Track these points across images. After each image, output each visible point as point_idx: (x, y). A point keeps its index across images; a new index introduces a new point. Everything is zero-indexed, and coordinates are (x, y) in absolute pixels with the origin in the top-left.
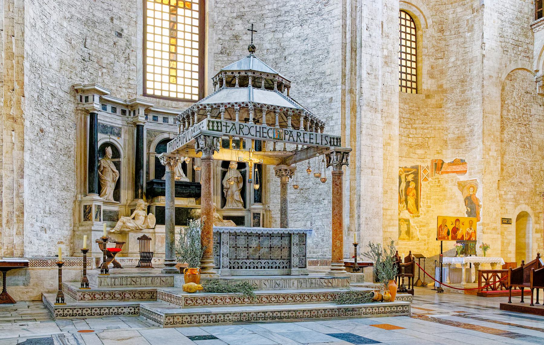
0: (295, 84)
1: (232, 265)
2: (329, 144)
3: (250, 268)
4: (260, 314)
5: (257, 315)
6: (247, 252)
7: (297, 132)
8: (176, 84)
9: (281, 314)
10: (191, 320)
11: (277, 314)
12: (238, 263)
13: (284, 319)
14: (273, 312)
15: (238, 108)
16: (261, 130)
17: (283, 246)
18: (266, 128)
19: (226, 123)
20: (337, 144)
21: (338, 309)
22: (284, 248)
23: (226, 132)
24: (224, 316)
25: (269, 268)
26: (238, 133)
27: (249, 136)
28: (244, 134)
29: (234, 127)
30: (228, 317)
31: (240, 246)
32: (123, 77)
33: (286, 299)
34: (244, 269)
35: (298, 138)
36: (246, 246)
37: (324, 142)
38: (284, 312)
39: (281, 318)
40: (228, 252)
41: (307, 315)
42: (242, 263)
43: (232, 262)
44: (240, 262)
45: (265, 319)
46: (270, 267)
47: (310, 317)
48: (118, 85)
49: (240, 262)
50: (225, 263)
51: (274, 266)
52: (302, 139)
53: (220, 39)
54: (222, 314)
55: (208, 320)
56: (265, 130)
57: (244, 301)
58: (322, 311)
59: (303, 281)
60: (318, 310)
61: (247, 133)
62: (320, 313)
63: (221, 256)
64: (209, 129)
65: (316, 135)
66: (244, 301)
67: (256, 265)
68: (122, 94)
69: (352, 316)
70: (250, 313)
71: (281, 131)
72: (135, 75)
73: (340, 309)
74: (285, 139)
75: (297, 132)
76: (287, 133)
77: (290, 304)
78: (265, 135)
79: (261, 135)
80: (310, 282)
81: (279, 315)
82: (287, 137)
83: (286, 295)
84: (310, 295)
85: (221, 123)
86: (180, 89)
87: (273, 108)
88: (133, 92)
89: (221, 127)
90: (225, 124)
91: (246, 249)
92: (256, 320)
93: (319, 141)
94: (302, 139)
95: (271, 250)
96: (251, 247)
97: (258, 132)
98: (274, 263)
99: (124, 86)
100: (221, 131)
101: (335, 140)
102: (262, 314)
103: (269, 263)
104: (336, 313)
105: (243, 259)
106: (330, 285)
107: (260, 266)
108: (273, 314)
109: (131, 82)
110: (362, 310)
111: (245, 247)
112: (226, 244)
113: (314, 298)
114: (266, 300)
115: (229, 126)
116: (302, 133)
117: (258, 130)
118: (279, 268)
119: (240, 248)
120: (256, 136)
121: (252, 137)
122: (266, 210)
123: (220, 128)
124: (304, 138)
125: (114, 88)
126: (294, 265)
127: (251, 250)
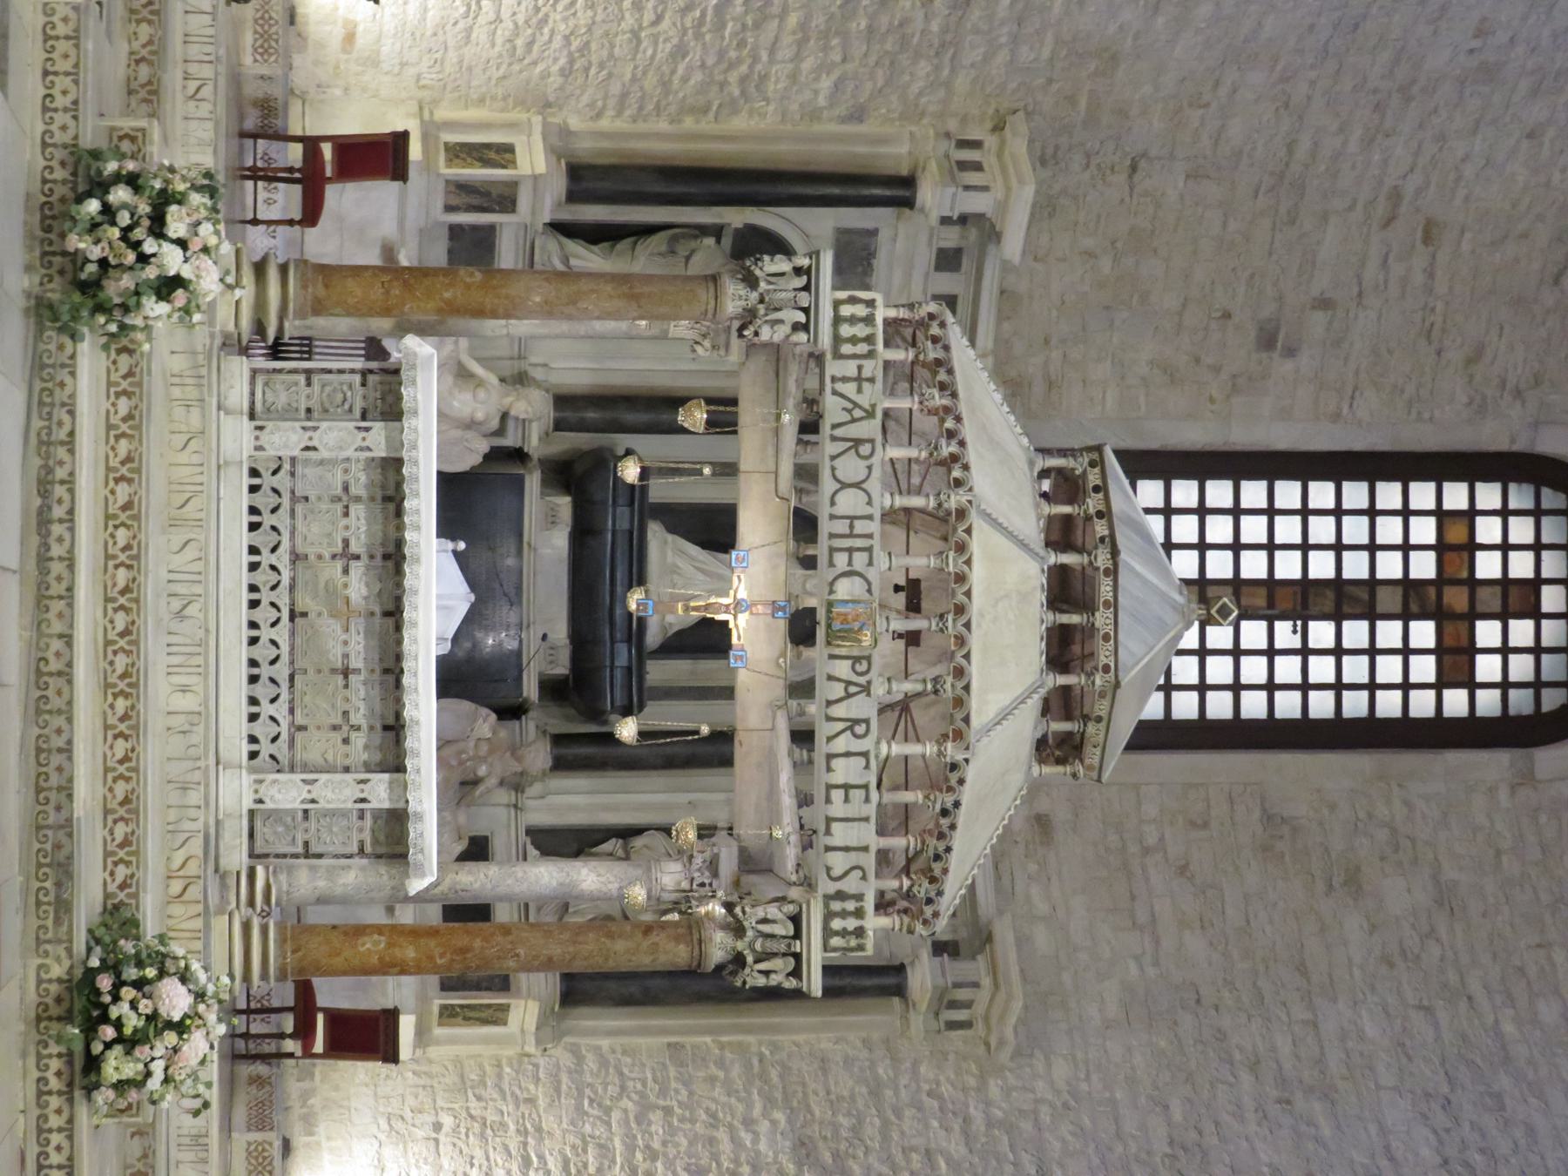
1: (267, 481)
2: (832, 888)
4: (66, 418)
5: (63, 405)
6: (327, 556)
7: (867, 721)
9: (61, 521)
10: (56, 110)
12: (274, 511)
13: (35, 540)
14: (70, 482)
16: (859, 543)
17: (353, 735)
18: (870, 564)
19: (872, 380)
20: (837, 933)
21: (69, 820)
22: (346, 741)
23: (834, 379)
25: (253, 663)
26: (839, 432)
27: (832, 486)
28: (833, 458)
29: (858, 413)
33: (122, 601)
34: (246, 538)
35: (841, 726)
37: (839, 862)
38: (67, 536)
40: (324, 454)
41: (50, 655)
42: (274, 528)
45: (41, 443)
46: (255, 671)
47: (39, 673)
49: (282, 520)
50: (276, 438)
53: (1333, 807)
57: (118, 395)
58: (65, 737)
59: (195, 738)
60: (68, 712)
61: (839, 474)
62: (59, 721)
63: (310, 424)
66: (118, 395)
67: (265, 596)
69: (32, 900)
70: (73, 374)
73: (70, 835)
74: (832, 657)
75: (867, 721)
78: (841, 560)
79: (838, 543)
80: (189, 777)
81: (58, 512)
83: (137, 601)
84: (136, 727)
85: (871, 354)
87: (961, 598)
89: (855, 356)
90: (866, 373)
91: (339, 549)
92: (41, 403)
95: (334, 671)
96: (346, 571)
97: (851, 527)
98: (273, 690)
99: (1056, 355)
102: (67, 428)
103: (273, 662)
104: (50, 808)
105: (293, 533)
106: (176, 887)
107: (257, 615)
108: (62, 482)
110: (58, 960)
111: (346, 542)
112: (359, 443)
114: (121, 502)
115: (859, 390)
117: (860, 527)
119: (344, 522)
120: (832, 517)
121: (827, 501)
123: (846, 349)
124: (848, 754)
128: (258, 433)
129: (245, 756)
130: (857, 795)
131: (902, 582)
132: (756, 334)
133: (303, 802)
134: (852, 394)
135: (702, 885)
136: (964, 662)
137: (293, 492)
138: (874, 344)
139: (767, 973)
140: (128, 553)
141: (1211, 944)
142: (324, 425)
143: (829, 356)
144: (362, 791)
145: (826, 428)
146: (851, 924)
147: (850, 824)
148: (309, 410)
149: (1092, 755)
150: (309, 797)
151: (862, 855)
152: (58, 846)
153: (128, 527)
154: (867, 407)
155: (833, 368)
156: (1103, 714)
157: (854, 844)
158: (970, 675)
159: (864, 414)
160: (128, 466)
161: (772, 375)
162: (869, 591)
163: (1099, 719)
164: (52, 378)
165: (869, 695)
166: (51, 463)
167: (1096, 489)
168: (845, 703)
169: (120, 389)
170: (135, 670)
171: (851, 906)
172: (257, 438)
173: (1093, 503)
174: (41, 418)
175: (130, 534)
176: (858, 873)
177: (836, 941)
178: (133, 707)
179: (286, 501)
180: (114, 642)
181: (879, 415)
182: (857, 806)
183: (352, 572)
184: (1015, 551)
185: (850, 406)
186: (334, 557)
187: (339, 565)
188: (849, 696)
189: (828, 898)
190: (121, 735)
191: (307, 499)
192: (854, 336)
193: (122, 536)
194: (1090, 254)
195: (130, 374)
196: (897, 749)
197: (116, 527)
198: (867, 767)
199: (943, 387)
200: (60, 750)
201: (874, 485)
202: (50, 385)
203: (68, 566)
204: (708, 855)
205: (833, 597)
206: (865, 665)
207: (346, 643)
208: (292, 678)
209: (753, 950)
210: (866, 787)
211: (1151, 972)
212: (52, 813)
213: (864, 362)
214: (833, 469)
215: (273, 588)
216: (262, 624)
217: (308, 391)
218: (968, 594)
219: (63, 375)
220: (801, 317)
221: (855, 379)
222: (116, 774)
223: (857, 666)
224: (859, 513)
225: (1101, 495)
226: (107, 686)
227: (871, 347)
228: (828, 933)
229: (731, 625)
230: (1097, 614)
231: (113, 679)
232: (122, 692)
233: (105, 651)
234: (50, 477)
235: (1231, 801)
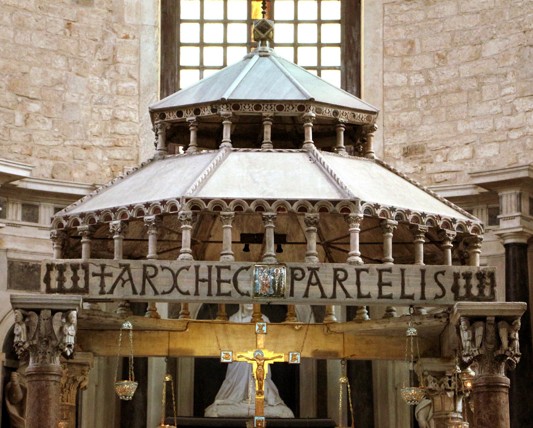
2: (450, 294)
7: (336, 270)
16: (214, 276)
18: (229, 268)
19: (103, 267)
26: (139, 289)
28: (156, 293)
29: (126, 276)
32: (95, 116)
35: (339, 288)
48: (78, 143)
61: (167, 289)
68: (92, 167)
72: (135, 107)
74: (292, 294)
76: (300, 275)
78: (226, 288)
79: (214, 290)
85: (85, 267)
87: (252, 207)
88: (128, 157)
89: (86, 278)
90: (98, 270)
94: (352, 288)
97: (203, 280)
99: (98, 142)
109: (121, 127)
115: (110, 275)
116: (351, 271)
117: (203, 275)
120: (197, 293)
121: (185, 297)
123: (81, 284)
124: (358, 284)
125: (62, 154)
130: (386, 277)
131: (243, 246)
132: (69, 346)
134: (114, 279)
135: (450, 383)
136: (295, 205)
138: (78, 265)
139: (511, 341)
141: (492, 38)
143: (86, 296)
145: (137, 297)
146: (474, 282)
147: (406, 283)
149: (361, 118)
151: (427, 274)
155: (94, 293)
156: (332, 110)
157: (420, 279)
158: (304, 200)
159: (126, 273)
161: (102, 334)
162: (247, 268)
163: (336, 113)
165: (317, 269)
168: (323, 285)
171: (462, 282)
173: (190, 117)
176: (440, 277)
177: (487, 292)
181: (127, 261)
182: (394, 278)
184: (221, 170)
185: (121, 282)
188: (318, 283)
192: (72, 278)
194: (27, 118)
196: (356, 249)
198: (367, 270)
199: (109, 218)
201: (175, 265)
204: (430, 378)
205: (251, 294)
206: (296, 272)
209: (494, 350)
210: (380, 271)
211: (511, 78)
213: (91, 272)
214: (164, 293)
218: (249, 201)
221: (102, 278)
223: (298, 277)
224: (194, 276)
225: (184, 113)
227: (80, 267)
228: (480, 297)
229: (272, 362)
230: (264, 114)
235: (395, 26)
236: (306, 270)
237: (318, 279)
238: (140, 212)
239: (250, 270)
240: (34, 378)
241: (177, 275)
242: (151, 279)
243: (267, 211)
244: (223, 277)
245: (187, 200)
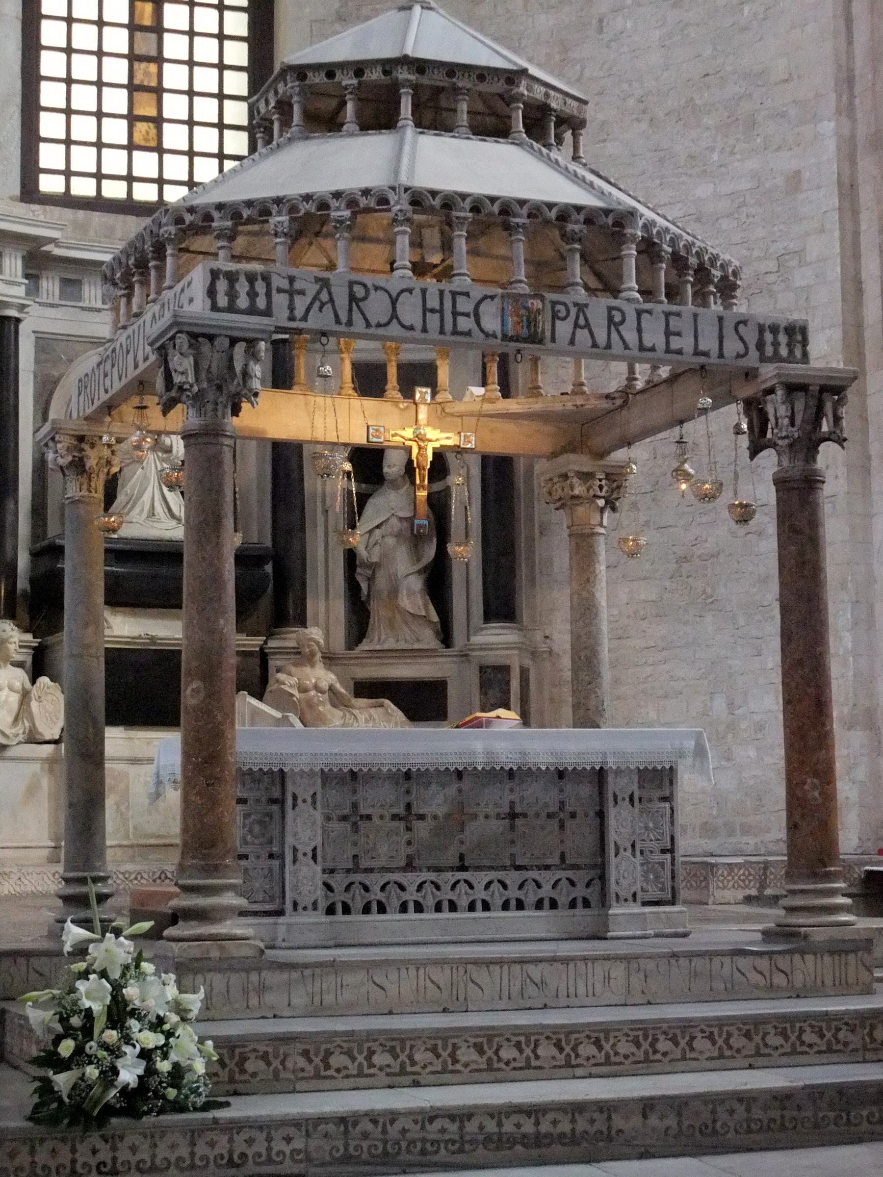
0: (644, 126)
1: (339, 897)
2: (754, 354)
3: (419, 908)
4: (438, 1124)
5: (423, 1127)
6: (407, 836)
8: (160, 150)
10: (114, 1159)
11: (518, 1126)
12: (366, 889)
15: (347, 213)
16: (448, 304)
18: (467, 294)
22: (573, 815)
24: (269, 1139)
25: (505, 906)
26: (344, 318)
27: (394, 325)
28: (368, 325)
29: (324, 296)
30: (288, 1140)
31: (375, 812)
35: (614, 336)
36: (400, 810)
37: (732, 346)
39: (538, 1141)
40: (318, 841)
42: (383, 888)
43: (338, 881)
44: (375, 881)
45: (461, 1151)
49: (375, 881)
50: (304, 889)
51: (531, 898)
52: (631, 337)
54: (261, 1128)
55: (192, 1154)
56: (465, 306)
57: (371, 1065)
58: (736, 1105)
63: (289, 858)
64: (215, 308)
65: (695, 316)
67: (446, 895)
71: (537, 304)
74: (553, 339)
75: (610, 309)
77: (591, 1076)
78: (464, 324)
79: (449, 327)
81: (528, 1127)
82: (564, 329)
85: (266, 278)
86: (175, 168)
87: (496, 208)
89: (268, 295)
90: (285, 284)
91: (401, 825)
93: (709, 343)
94: (631, 337)
95: (512, 827)
96: (422, 817)
97: (433, 311)
100: (267, 312)
101: (783, 339)
102: (447, 1123)
103: (505, 886)
107: (464, 902)
108: (500, 1124)
111: (395, 817)
113: (701, 1044)
115: (302, 293)
116: (630, 311)
117: (433, 302)
118: (554, 905)
119: (375, 819)
120: (424, 330)
122: (534, 654)
123: (261, 303)
124: (639, 331)
126: (622, 894)
127: (422, 829)
128: (300, 908)
129: (587, 911)
133: (634, 856)
134: (308, 300)
135: (601, 487)
137: (348, 871)
138: (256, 274)
140: (523, 1046)
142: (289, 840)
144: (624, 799)
148: (271, 856)
150: (630, 850)
151: (725, 324)
152: (832, 1106)
153: (499, 1047)
154: (318, 287)
158: (567, 205)
159: (325, 292)
160: (440, 1051)
162: (492, 298)
164: (397, 1143)
165: (586, 306)
166: (481, 1137)
167: (330, 75)
168: (594, 330)
169: (365, 1063)
170: (631, 1033)
172: (305, 908)
174: (437, 1152)
175: (505, 1043)
176: (741, 328)
178: (665, 1033)
179: (358, 877)
180: (607, 1056)
183: (421, 812)
185: (317, 304)
186: (409, 829)
187: (417, 824)
188: (587, 325)
189: (763, 359)
190: (690, 1044)
191: (355, 857)
192: (248, 294)
193: (507, 1053)
195: (349, 1054)
197: (499, 1060)
198: (649, 312)
200: (748, 1110)
202: (404, 1144)
203: (581, 1113)
205: (499, 335)
206: (559, 307)
207: (487, 817)
208: (518, 868)
212: (803, 1114)
213: (274, 286)
214: (379, 325)
215: (438, 888)
216: (471, 899)
217: (252, 858)
218: (493, 199)
219: (393, 1131)
220: (240, 349)
222: (725, 1047)
223: (560, 315)
226: (647, 1060)
227: (259, 278)
229: (437, 445)
230: (460, 85)
231: (640, 1055)
232: (652, 1045)
233: (616, 1064)
234: (495, 1138)
236: (571, 306)
237: (586, 319)
238: (324, 206)
239: (496, 300)
240: (200, 440)
241: (397, 299)
242: (361, 304)
243: (514, 216)
244: (460, 308)
245: (406, 190)
